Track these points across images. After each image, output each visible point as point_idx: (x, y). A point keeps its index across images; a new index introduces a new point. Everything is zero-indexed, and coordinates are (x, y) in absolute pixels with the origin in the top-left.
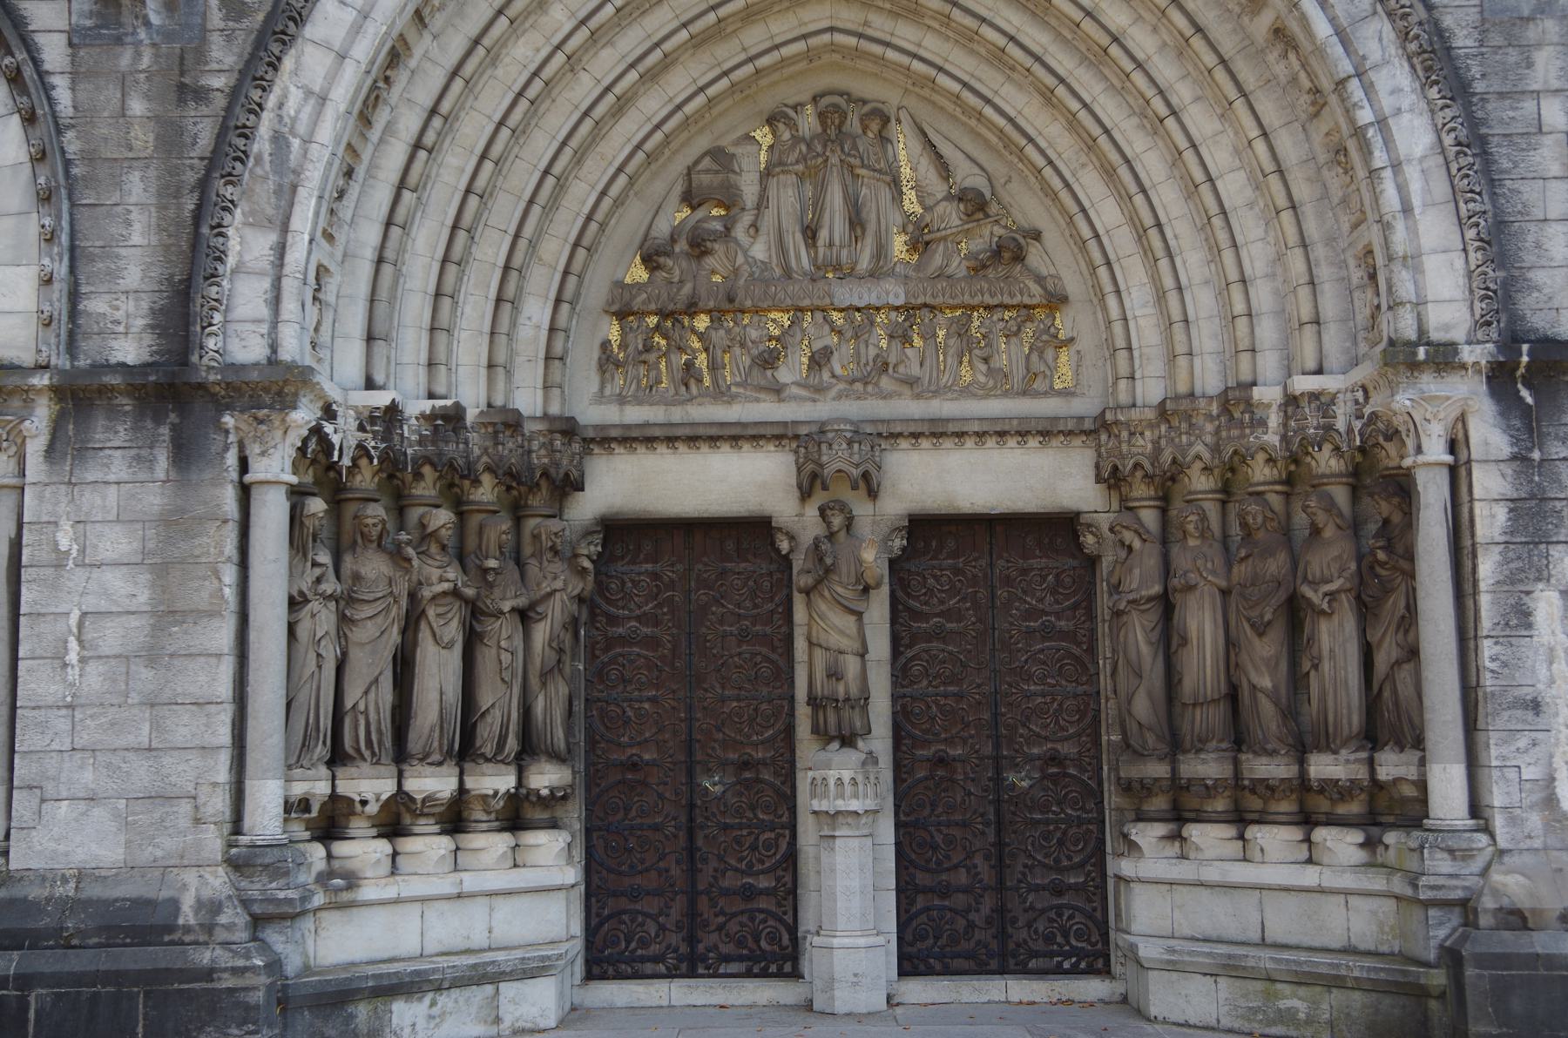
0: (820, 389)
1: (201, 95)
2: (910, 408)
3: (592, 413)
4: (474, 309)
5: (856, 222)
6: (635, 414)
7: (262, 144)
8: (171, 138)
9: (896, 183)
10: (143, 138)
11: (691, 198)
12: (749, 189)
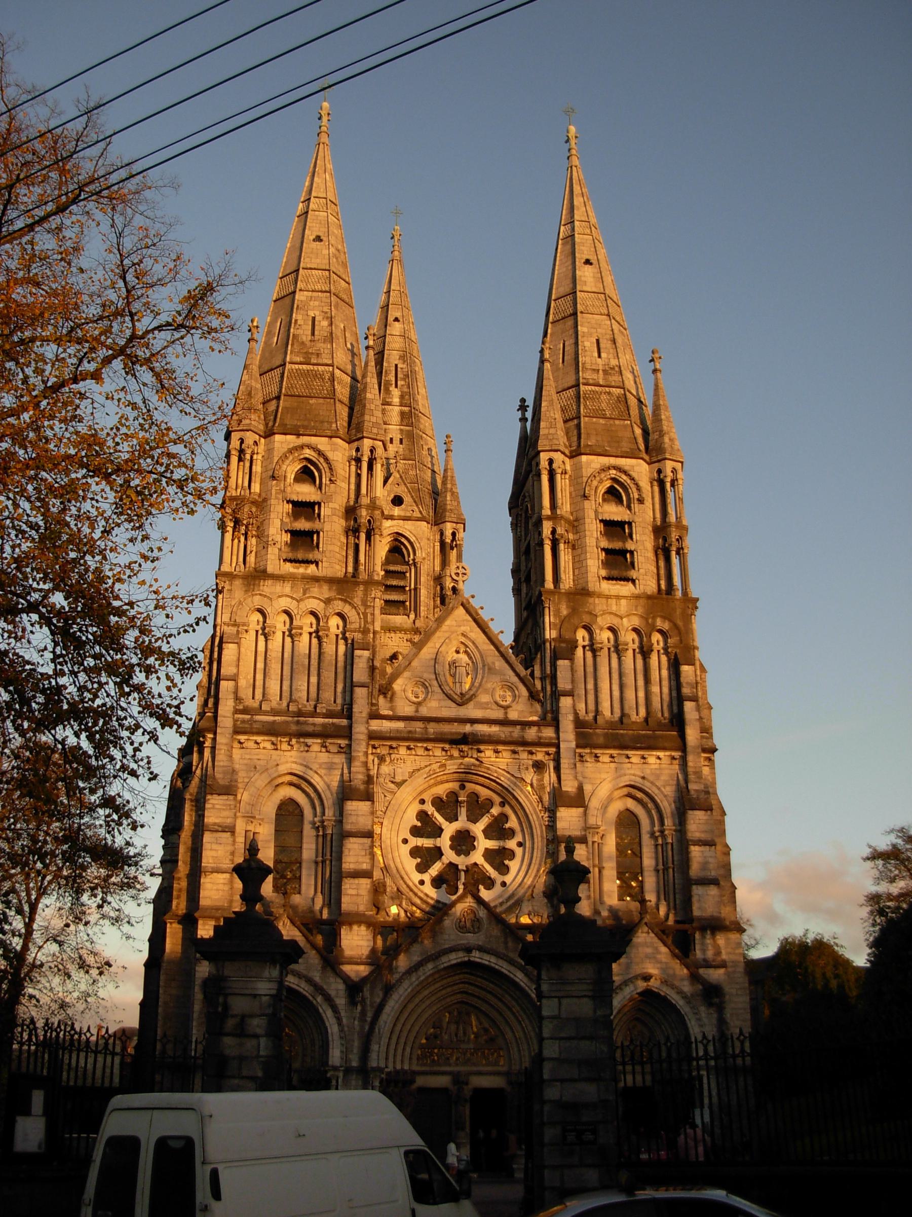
0: (457, 1065)
1: (366, 1021)
2: (474, 1069)
3: (416, 1068)
4: (400, 1051)
5: (465, 1033)
6: (423, 1069)
7: (377, 1030)
8: (362, 1027)
9: (472, 1025)
10: (357, 1028)
11: (433, 1028)
12: (445, 1025)
